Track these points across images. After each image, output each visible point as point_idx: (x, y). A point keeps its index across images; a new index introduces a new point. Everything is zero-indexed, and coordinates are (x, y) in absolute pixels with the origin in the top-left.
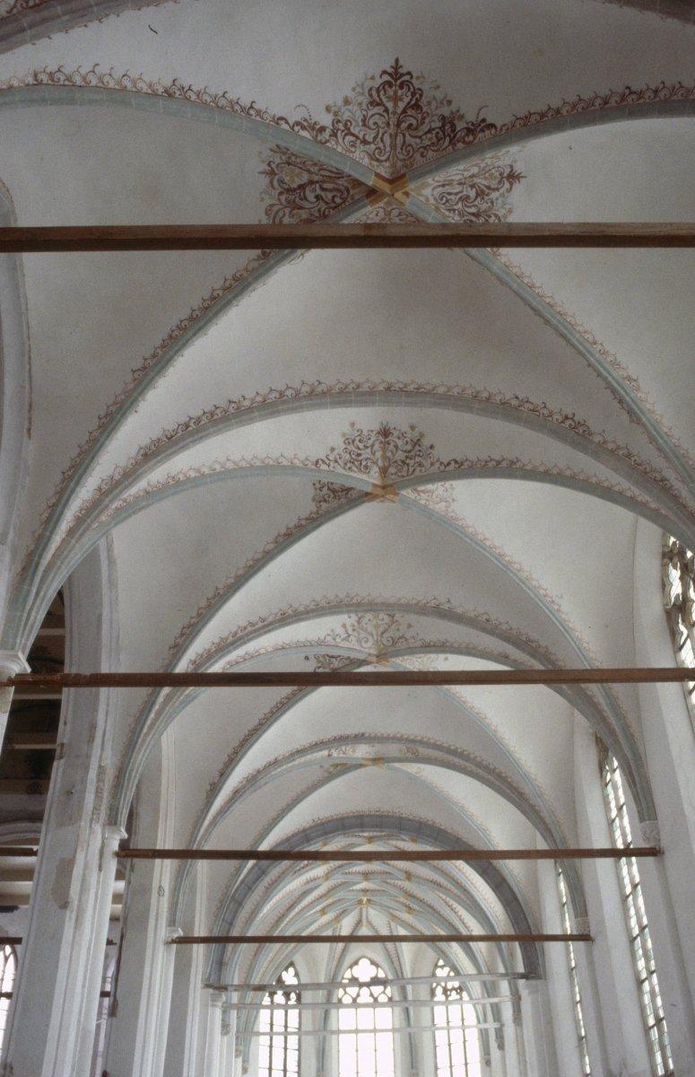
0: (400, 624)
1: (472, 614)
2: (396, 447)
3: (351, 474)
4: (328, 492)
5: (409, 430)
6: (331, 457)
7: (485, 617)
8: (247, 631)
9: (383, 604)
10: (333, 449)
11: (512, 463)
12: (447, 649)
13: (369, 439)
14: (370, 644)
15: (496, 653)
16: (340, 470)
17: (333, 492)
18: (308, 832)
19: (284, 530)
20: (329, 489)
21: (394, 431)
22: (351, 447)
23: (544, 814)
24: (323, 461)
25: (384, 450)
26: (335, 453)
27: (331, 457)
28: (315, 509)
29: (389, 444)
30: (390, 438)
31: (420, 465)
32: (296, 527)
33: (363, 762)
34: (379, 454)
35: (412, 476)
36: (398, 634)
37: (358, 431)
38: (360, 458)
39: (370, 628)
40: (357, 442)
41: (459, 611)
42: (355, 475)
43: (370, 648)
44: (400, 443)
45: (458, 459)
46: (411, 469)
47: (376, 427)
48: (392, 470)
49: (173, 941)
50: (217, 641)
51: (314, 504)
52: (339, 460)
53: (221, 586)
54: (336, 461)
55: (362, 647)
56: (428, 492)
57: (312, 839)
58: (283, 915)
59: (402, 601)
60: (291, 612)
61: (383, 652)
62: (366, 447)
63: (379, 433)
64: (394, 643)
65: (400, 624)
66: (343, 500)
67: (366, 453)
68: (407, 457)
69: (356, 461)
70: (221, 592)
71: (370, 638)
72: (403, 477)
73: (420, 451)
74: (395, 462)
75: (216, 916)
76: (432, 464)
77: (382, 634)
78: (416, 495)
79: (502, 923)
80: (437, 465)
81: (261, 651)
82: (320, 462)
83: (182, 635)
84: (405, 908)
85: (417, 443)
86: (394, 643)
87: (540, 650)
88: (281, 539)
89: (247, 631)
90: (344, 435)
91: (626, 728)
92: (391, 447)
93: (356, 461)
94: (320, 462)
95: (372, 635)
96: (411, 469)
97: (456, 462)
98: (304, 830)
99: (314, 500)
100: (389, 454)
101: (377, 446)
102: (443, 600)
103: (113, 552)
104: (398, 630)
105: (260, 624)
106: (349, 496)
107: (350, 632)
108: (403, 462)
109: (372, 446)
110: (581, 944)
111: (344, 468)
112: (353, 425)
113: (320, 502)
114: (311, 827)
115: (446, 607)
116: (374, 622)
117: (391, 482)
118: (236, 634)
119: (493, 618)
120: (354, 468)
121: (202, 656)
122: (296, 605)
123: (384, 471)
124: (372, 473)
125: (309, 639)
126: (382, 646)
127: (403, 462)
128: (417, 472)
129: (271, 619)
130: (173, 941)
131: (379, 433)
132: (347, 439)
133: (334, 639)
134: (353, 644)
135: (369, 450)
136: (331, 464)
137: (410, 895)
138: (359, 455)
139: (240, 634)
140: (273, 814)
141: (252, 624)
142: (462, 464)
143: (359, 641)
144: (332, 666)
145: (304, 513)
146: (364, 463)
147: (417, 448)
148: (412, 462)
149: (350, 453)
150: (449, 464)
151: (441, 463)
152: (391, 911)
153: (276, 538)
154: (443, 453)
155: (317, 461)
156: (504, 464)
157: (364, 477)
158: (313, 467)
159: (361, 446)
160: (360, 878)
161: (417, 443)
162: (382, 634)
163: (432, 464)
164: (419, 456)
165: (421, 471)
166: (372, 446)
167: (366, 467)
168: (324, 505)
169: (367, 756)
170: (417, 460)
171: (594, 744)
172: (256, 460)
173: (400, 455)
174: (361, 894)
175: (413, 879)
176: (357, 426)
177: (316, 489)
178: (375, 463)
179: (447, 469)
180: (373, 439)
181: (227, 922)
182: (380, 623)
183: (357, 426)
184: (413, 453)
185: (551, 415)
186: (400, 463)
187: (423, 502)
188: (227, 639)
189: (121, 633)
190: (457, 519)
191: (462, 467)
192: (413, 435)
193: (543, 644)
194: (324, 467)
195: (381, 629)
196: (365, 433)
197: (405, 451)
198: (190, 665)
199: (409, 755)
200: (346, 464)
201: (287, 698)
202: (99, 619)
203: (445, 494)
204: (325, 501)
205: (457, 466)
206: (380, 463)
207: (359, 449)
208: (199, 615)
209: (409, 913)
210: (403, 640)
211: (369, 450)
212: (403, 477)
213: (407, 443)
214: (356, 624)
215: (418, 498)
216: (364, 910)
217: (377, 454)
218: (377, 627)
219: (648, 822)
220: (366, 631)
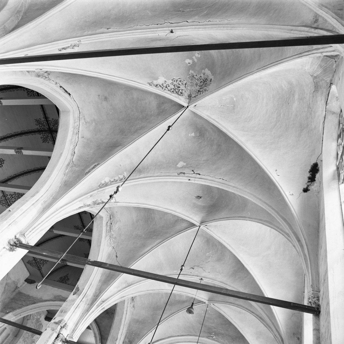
6: (165, 85)
24: (160, 85)
38: (179, 89)
46: (201, 93)
52: (168, 87)
67: (182, 87)
82: (158, 86)
94: (158, 86)
127: (199, 91)
132: (174, 79)
138: (179, 87)
146: (180, 91)
149: (174, 86)
155: (157, 85)
159: (180, 83)
164: (205, 86)
184: (203, 86)
200: (171, 89)
207: (179, 85)
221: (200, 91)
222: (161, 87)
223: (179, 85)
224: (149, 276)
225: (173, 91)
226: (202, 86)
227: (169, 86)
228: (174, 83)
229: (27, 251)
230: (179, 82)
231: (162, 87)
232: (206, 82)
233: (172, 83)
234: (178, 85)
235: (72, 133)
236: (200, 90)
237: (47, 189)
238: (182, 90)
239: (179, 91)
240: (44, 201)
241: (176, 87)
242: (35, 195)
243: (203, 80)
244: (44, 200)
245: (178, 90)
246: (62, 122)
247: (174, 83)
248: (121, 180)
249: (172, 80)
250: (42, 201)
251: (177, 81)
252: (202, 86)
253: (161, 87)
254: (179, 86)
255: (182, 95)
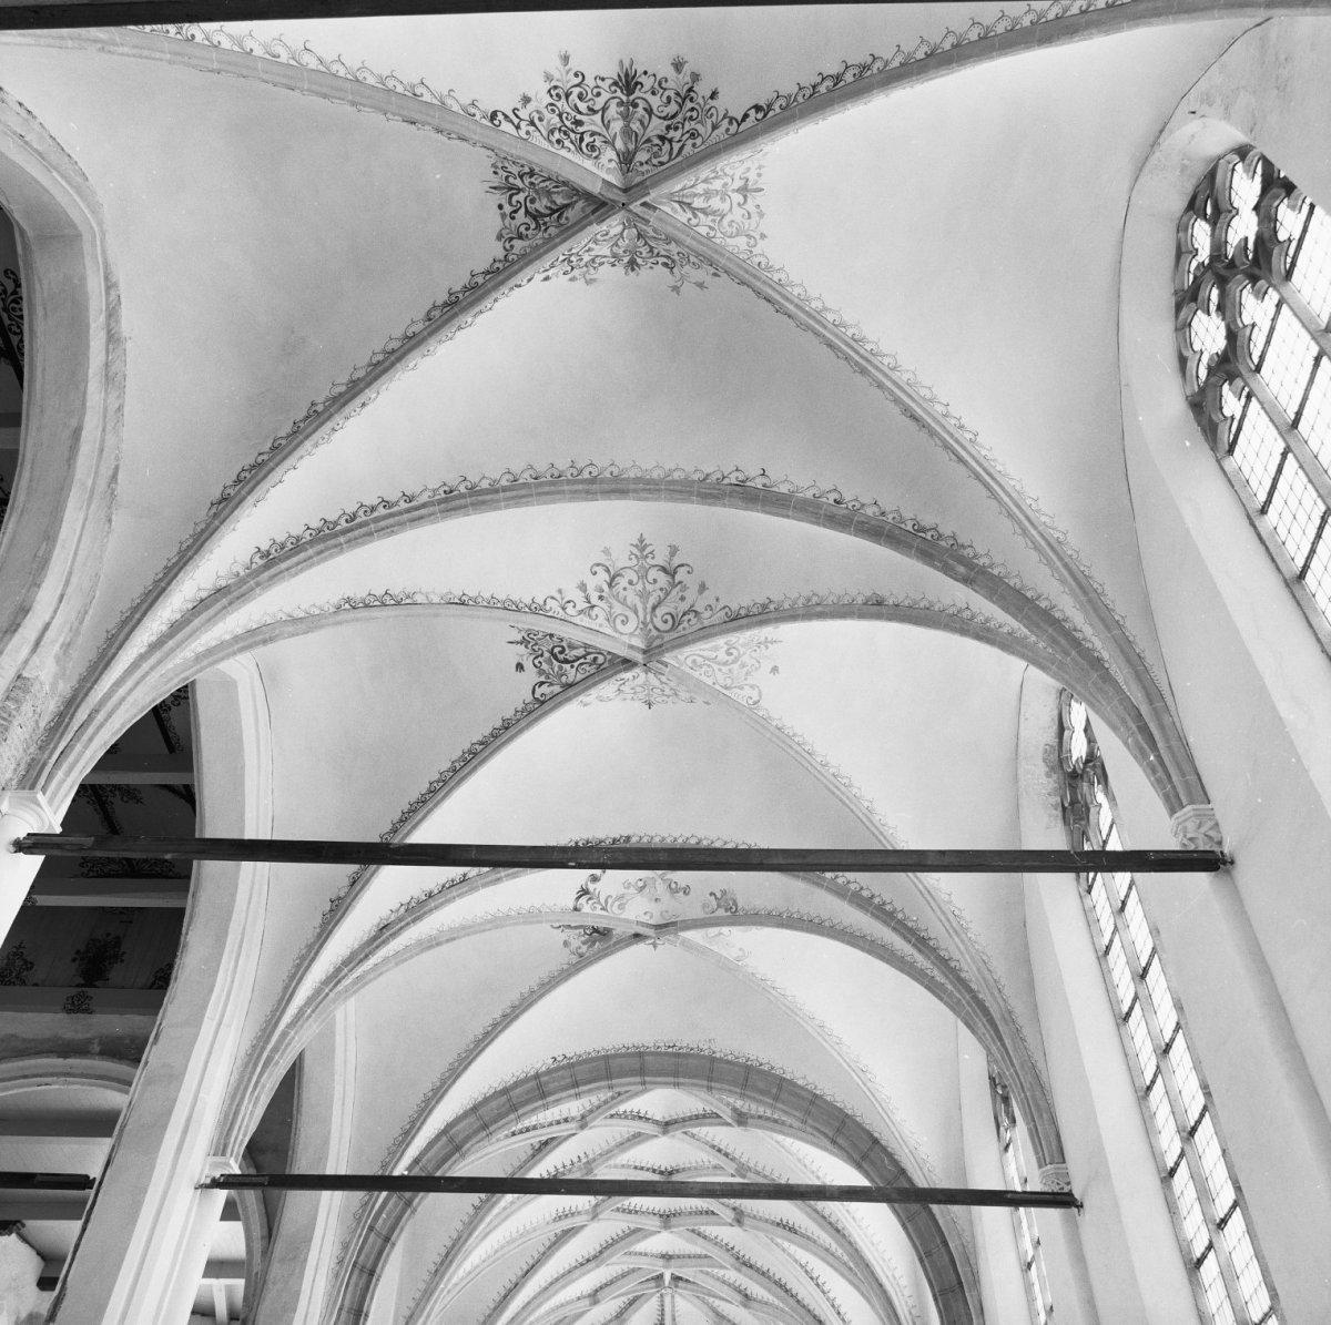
0: (685, 588)
1: (809, 494)
2: (649, 111)
3: (563, 152)
4: (528, 220)
5: (670, 72)
7: (833, 496)
8: (376, 514)
9: (637, 480)
10: (526, 100)
11: (865, 67)
12: (771, 616)
13: (599, 94)
14: (632, 625)
15: (860, 600)
16: (538, 140)
17: (535, 218)
18: (544, 1079)
19: (442, 297)
20: (527, 212)
21: (643, 79)
22: (561, 104)
23: (970, 972)
24: (506, 116)
25: (626, 117)
26: (531, 107)
27: (524, 114)
28: (500, 254)
29: (635, 106)
30: (637, 93)
31: (693, 135)
32: (465, 289)
33: (641, 930)
34: (617, 126)
35: (679, 159)
36: (684, 606)
37: (576, 75)
38: (581, 129)
39: (632, 598)
40: (574, 97)
41: (784, 489)
42: (569, 156)
43: (631, 634)
44: (655, 102)
45: (762, 103)
46: (676, 147)
47: (612, 71)
48: (642, 156)
49: (216, 1184)
50: (316, 524)
51: (500, 244)
52: (536, 121)
53: (320, 399)
54: (532, 123)
55: (616, 631)
56: (714, 213)
57: (550, 1094)
58: (517, 1285)
59: (676, 475)
60: (463, 490)
61: (655, 644)
62: (592, 111)
63: (615, 84)
64: (676, 623)
65: (685, 588)
66: (552, 231)
67: (592, 123)
68: (668, 128)
69: (569, 130)
70: (320, 408)
71: (631, 615)
72: (662, 164)
73: (692, 109)
74: (648, 140)
75: (359, 1220)
76: (715, 127)
77: (654, 608)
78: (690, 215)
79: (907, 1292)
80: (725, 123)
81: (419, 599)
82: (500, 117)
83: (238, 481)
84: (739, 1298)
85: (687, 95)
86: (676, 623)
87: (943, 543)
88: (437, 313)
89: (376, 514)
90: (549, 78)
91: (1125, 647)
92: (640, 109)
93: (569, 130)
94: (500, 117)
95: (636, 612)
96: (676, 147)
97: (758, 108)
98: (537, 1076)
99: (499, 237)
100: (635, 126)
101: (613, 110)
102: (753, 471)
103: (117, 322)
104: (683, 599)
105: (403, 505)
106: (563, 221)
107: (594, 600)
108: (662, 138)
109: (604, 109)
110: (1053, 1214)
111: (550, 141)
112: (566, 59)
113: (511, 239)
114: (549, 1072)
115: (759, 483)
116: (639, 587)
117: (638, 179)
118: (353, 517)
119: (848, 497)
120: (567, 143)
121: (283, 546)
122: (473, 478)
123: (626, 159)
124: (604, 160)
125: (515, 598)
126: (655, 633)
127: (662, 138)
128: (688, 149)
129: (424, 498)
130: (216, 1184)
131: (615, 84)
132: (556, 87)
133: (564, 609)
134: (599, 621)
135: (597, 117)
136: (523, 124)
137: (744, 1264)
139: (361, 518)
140: (477, 1029)
141: (387, 504)
142: (770, 106)
143: (610, 619)
144: (564, 679)
145: (482, 264)
146: (587, 139)
147: (689, 105)
148: (676, 135)
149: (560, 116)
150: (746, 116)
151: (732, 120)
152: (717, 1303)
153: (429, 312)
154: (734, 101)
155: (494, 115)
156: (849, 77)
157: (588, 164)
158: (486, 122)
159: (582, 106)
160: (655, 1223)
161: (687, 95)
162: (654, 608)
163: (715, 127)
164: (691, 118)
165: (694, 145)
166: (604, 109)
167: (592, 147)
168: (518, 244)
169: (645, 919)
170: (687, 127)
171: (1060, 823)
172: (367, 75)
173: (657, 127)
174: (661, 1262)
175: (747, 1221)
176: (574, 65)
177: (503, 216)
178: (610, 143)
179: (742, 128)
180: (605, 96)
181: (378, 1234)
182: (650, 587)
183: (574, 65)
184: (679, 118)
185: (973, 617)
186: (657, 141)
187: (703, 230)
188: (336, 523)
189: (257, 778)
190: (769, 268)
191: (771, 114)
192: (676, 82)
193: (946, 530)
194: (506, 127)
195: (652, 601)
196: (590, 81)
197: (664, 118)
198: (257, 559)
199: (721, 912)
200: (552, 132)
201: (481, 743)
202: (76, 434)
203: (747, 222)
204: (520, 237)
205: (760, 116)
206: (619, 144)
207: (580, 113)
208: (274, 448)
209: (745, 1306)
210: (691, 616)
211: (597, 117)
212: (662, 164)
213: (669, 99)
214: (605, 587)
215: (694, 221)
216: (667, 1300)
217: (612, 125)
218: (644, 595)
219: (1189, 808)
220: (623, 602)
221: (670, 141)
222: (511, 121)
223: (580, 113)
224: (502, 857)
225: (558, 141)
226: (673, 117)
227: (541, 120)
228: (559, 104)
229: (42, 858)
230: (577, 101)
231: (516, 121)
232: (691, 100)
233: (552, 104)
234: (574, 114)
235: (103, 335)
236: (669, 136)
237: (59, 592)
238: (592, 135)
239: (582, 140)
240: (62, 646)
241: (568, 123)
242: (19, 625)
243: (678, 94)
244: (61, 639)
245: (578, 136)
246: (45, 287)
247: (559, 104)
248: (353, 520)
249: (549, 91)
250: (58, 645)
251: (567, 96)
252: (673, 117)
253: (511, 121)
254: (579, 117)
255: (594, 154)
